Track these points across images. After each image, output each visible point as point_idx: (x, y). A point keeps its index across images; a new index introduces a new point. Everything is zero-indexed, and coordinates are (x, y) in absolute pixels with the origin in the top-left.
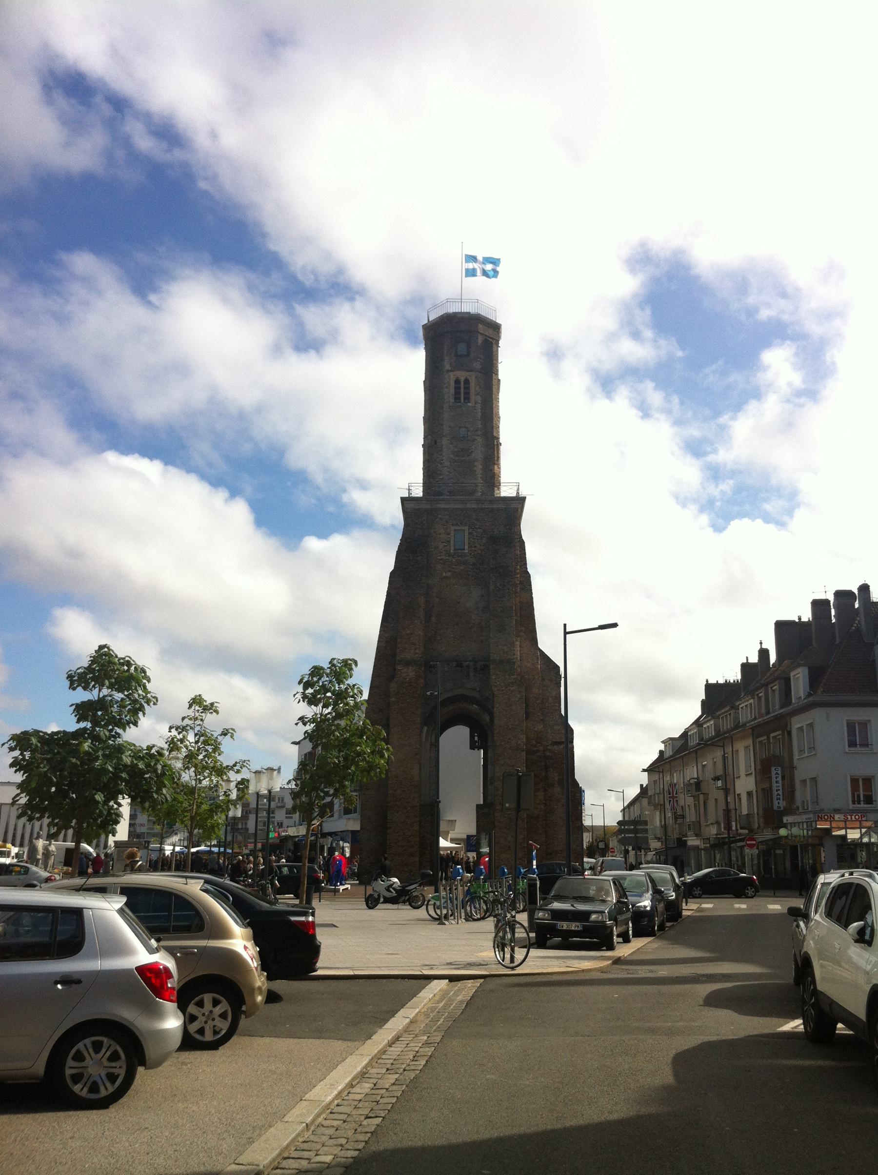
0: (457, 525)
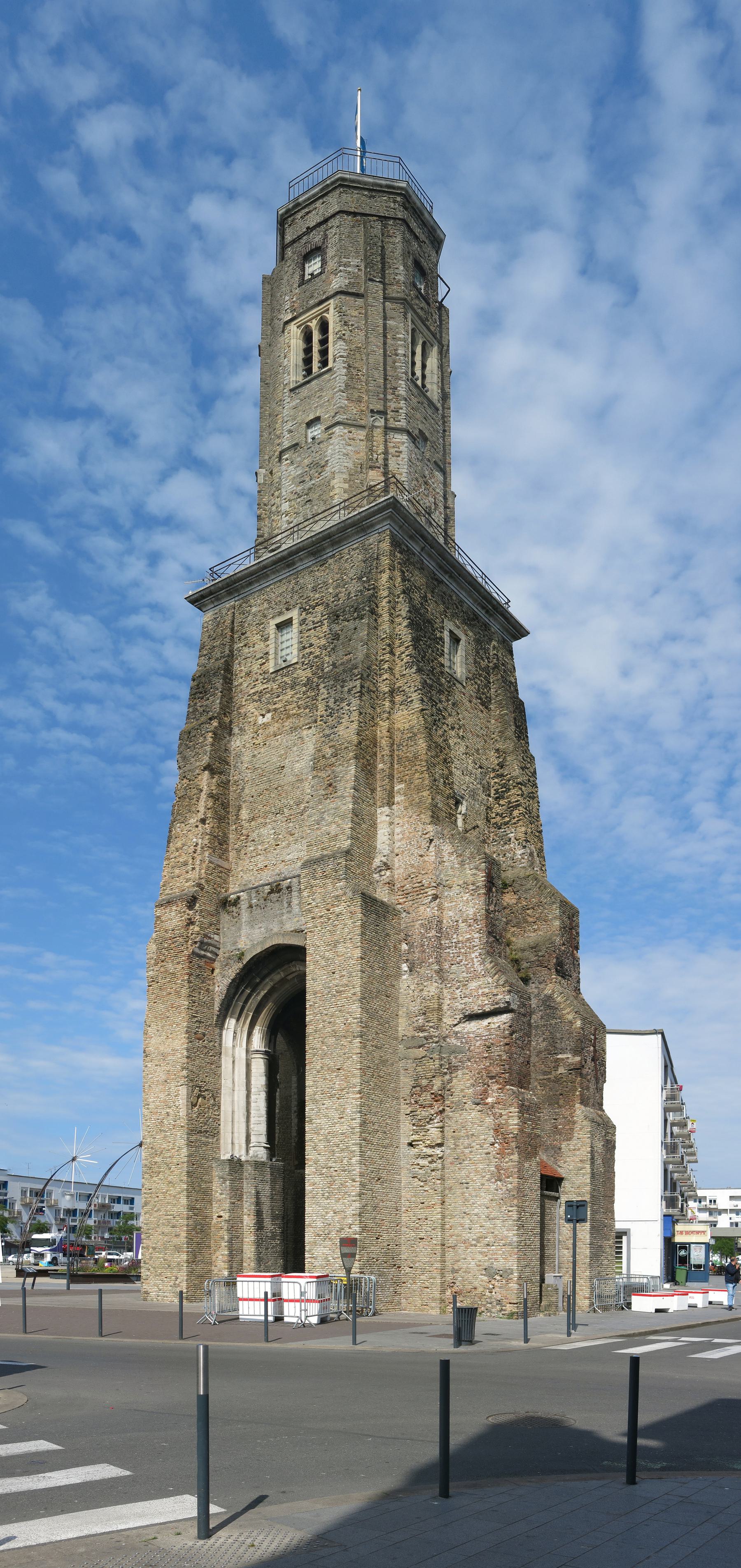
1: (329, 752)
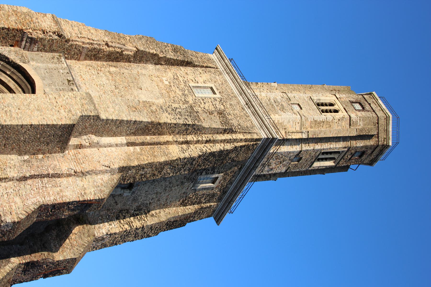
0: (218, 89)
1: (154, 108)
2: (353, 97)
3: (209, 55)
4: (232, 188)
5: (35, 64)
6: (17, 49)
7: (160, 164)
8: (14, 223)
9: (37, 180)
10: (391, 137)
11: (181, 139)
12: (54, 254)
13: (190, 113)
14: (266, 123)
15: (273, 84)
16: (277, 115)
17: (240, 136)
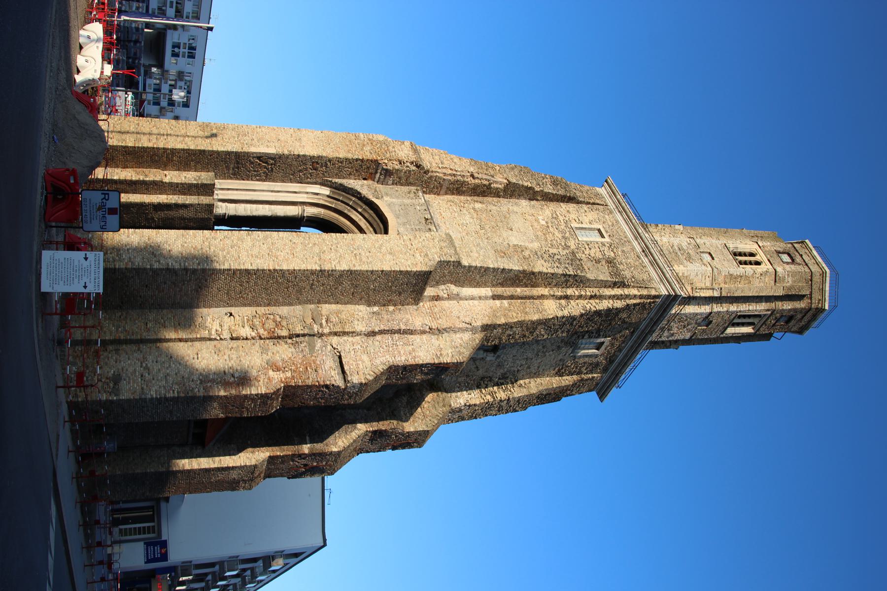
0: (607, 232)
1: (527, 253)
2: (780, 246)
3: (597, 189)
4: (621, 356)
5: (390, 200)
6: (370, 182)
7: (533, 322)
8: (361, 384)
9: (386, 336)
10: (827, 298)
11: (559, 292)
12: (405, 424)
13: (572, 260)
14: (668, 276)
15: (677, 227)
16: (681, 266)
17: (634, 292)
